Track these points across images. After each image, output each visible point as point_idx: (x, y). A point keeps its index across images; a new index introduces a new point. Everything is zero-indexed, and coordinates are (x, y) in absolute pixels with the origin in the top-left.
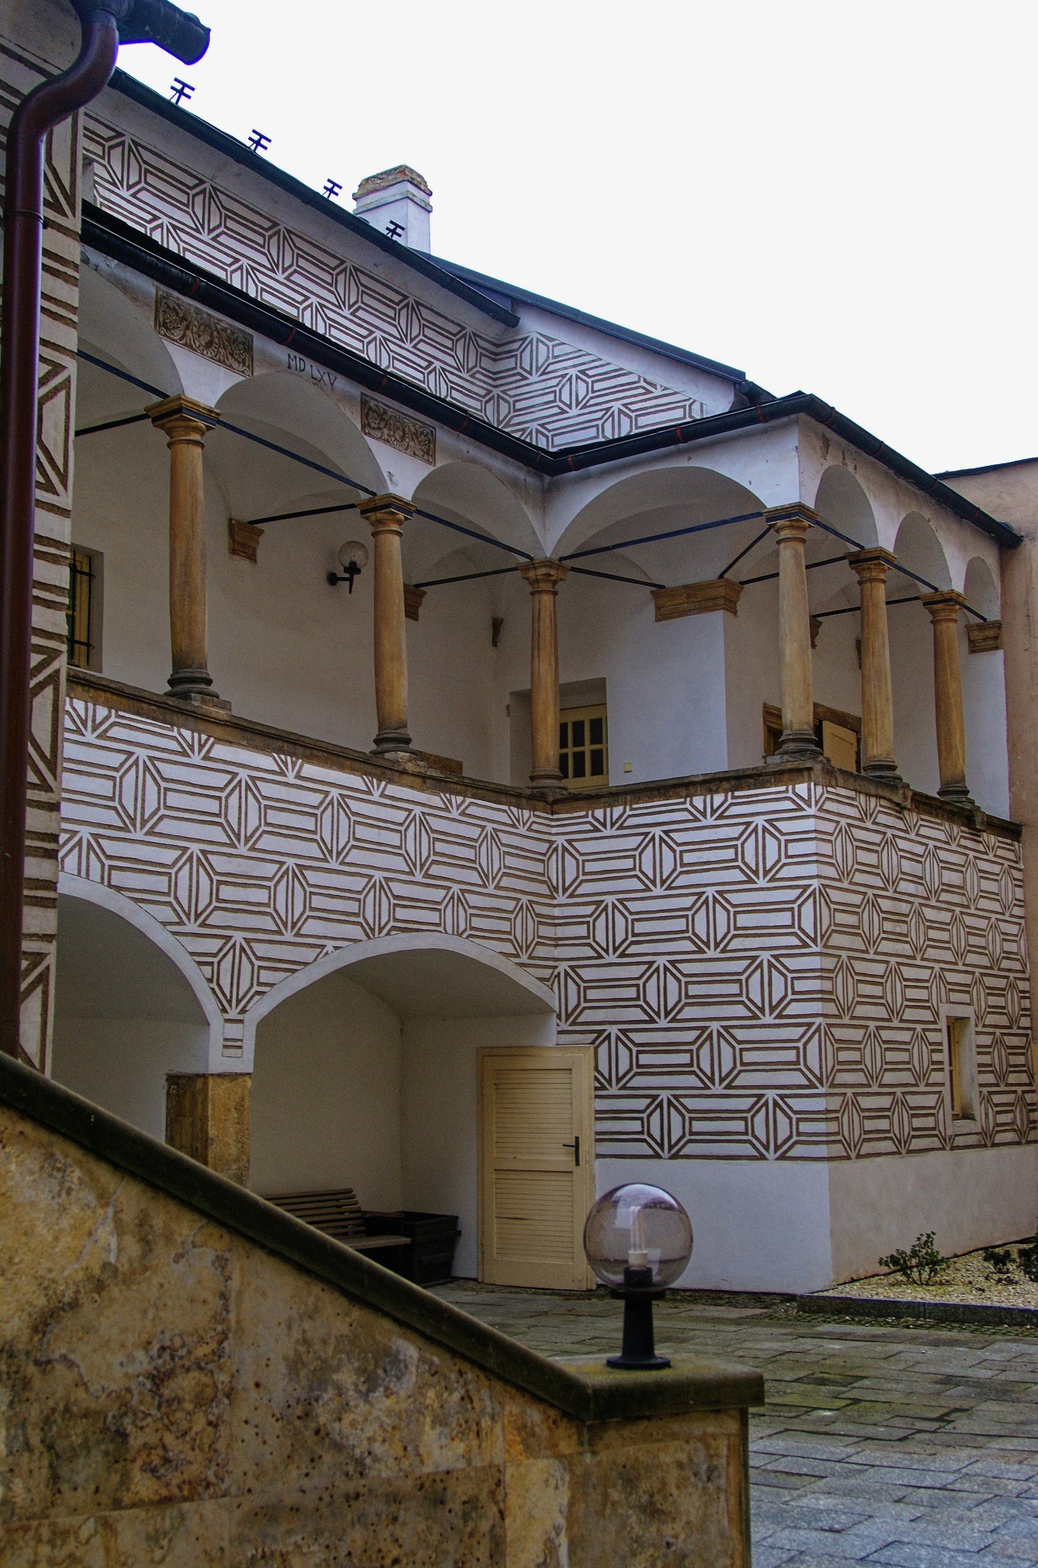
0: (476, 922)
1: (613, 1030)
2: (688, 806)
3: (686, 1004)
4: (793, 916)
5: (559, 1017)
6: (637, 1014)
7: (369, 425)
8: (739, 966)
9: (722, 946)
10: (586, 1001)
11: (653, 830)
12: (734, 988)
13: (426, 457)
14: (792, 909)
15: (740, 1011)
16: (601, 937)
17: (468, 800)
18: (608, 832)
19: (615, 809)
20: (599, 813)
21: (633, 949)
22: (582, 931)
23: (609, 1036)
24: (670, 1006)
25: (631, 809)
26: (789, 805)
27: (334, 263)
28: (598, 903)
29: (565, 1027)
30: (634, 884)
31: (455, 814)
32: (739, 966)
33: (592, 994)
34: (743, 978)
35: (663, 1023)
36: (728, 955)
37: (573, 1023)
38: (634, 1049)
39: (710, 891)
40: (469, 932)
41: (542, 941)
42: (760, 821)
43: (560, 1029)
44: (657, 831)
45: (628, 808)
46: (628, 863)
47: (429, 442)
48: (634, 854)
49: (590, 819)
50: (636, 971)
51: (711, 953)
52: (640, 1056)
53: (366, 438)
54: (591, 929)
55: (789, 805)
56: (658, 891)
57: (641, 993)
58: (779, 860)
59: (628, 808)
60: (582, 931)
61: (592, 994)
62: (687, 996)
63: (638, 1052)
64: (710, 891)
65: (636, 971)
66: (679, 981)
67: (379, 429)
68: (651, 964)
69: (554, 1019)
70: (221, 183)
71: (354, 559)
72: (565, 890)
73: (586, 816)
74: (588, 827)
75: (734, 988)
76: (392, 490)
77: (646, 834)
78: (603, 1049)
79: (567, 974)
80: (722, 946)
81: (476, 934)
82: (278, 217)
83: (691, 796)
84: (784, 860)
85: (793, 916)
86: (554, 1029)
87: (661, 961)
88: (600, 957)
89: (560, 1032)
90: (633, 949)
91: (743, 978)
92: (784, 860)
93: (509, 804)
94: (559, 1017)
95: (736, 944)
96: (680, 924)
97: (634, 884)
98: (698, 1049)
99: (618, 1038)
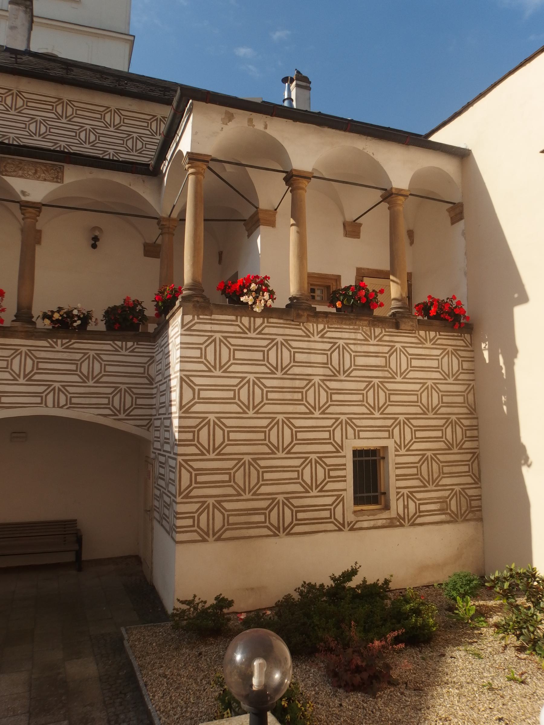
0: (74, 400)
7: (6, 171)
13: (55, 180)
17: (73, 341)
27: (102, 109)
31: (59, 348)
40: (69, 405)
41: (141, 406)
47: (58, 172)
53: (5, 177)
67: (14, 171)
70: (21, 88)
71: (96, 234)
76: (23, 198)
81: (72, 406)
82: (61, 95)
93: (113, 340)
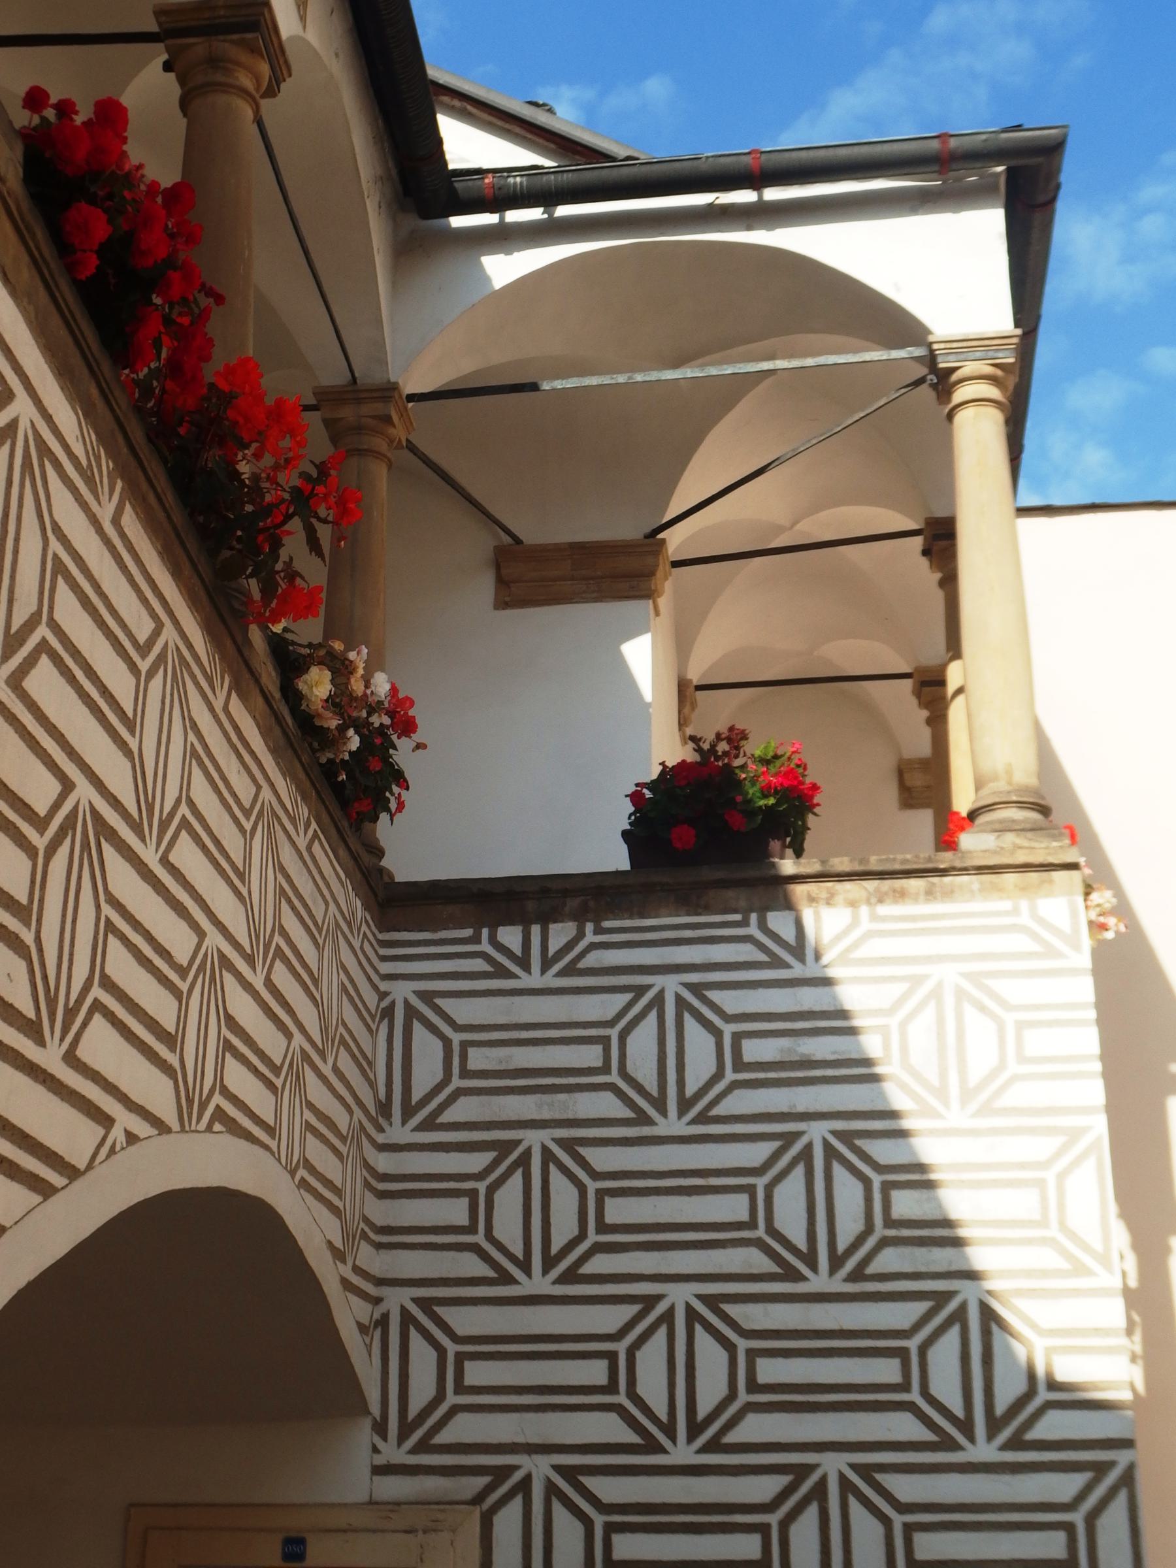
1: (540, 1468)
2: (753, 930)
3: (750, 1407)
4: (1044, 1199)
5: (380, 1428)
6: (607, 1428)
8: (901, 1315)
9: (850, 1265)
10: (460, 1388)
11: (658, 981)
12: (886, 1371)
14: (1041, 1184)
15: (905, 1427)
16: (508, 1227)
18: (535, 979)
19: (553, 928)
20: (511, 936)
21: (600, 1264)
22: (455, 1212)
23: (525, 1485)
24: (704, 1408)
25: (598, 931)
26: (1023, 943)
28: (505, 1148)
29: (393, 1453)
30: (606, 1105)
32: (901, 1315)
33: (476, 1374)
34: (913, 1344)
35: (682, 1453)
36: (865, 1284)
37: (423, 1446)
38: (599, 1520)
39: (817, 1132)
42: (949, 974)
43: (379, 1460)
44: (671, 984)
45: (589, 927)
46: (590, 1056)
48: (610, 1037)
49: (485, 947)
50: (610, 1318)
51: (819, 1282)
52: (616, 1538)
54: (482, 1210)
55: (1023, 943)
56: (672, 1124)
57: (621, 1376)
58: (1001, 1066)
59: (589, 927)
60: (455, 1212)
61: (476, 1374)
62: (753, 1386)
63: (610, 1529)
64: (817, 1132)
65: (610, 1318)
66: (730, 1347)
68: (650, 1302)
69: (363, 1433)
72: (408, 1111)
73: (476, 939)
74: (479, 965)
75: (886, 1371)
77: (640, 990)
78: (508, 1522)
79: (407, 1319)
80: (850, 1265)
83: (763, 910)
84: (1013, 1068)
85: (1044, 1199)
86: (362, 1461)
87: (680, 1295)
88: (509, 1280)
89: (378, 1470)
90: (600, 1264)
91: (913, 1344)
92: (1013, 1068)
94: (380, 1428)
95: (889, 1260)
96: (734, 1208)
97: (606, 1105)
98: (785, 1525)
99: (551, 1490)
